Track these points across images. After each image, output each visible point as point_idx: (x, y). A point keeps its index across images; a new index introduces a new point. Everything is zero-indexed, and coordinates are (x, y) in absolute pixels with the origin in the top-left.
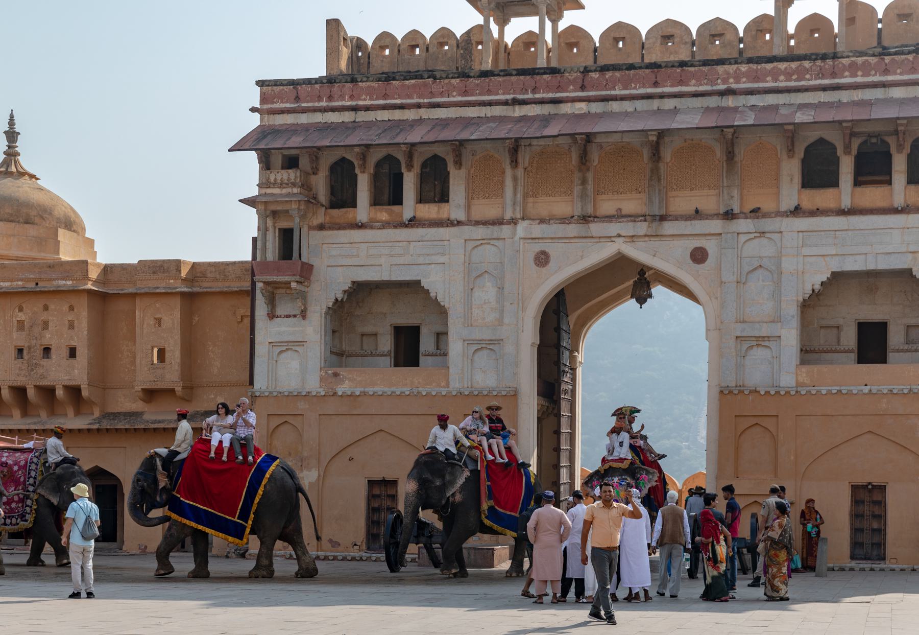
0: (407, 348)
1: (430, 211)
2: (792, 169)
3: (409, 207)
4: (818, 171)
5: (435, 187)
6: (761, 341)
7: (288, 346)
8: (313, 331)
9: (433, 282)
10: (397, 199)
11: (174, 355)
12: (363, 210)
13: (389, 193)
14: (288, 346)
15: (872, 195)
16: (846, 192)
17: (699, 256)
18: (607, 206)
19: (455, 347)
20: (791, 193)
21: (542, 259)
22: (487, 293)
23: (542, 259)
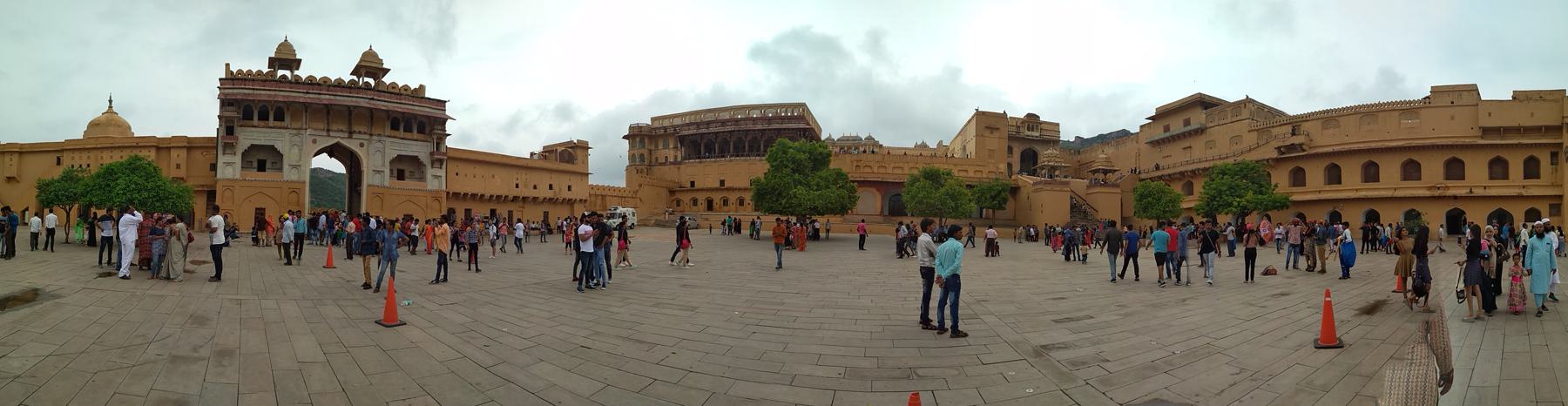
0: (262, 167)
1: (278, 124)
2: (388, 125)
3: (271, 122)
4: (395, 127)
5: (279, 117)
6: (378, 172)
7: (229, 164)
8: (238, 159)
9: (278, 146)
10: (267, 119)
11: (183, 166)
12: (256, 121)
13: (264, 117)
14: (229, 164)
15: (408, 135)
16: (401, 133)
17: (362, 145)
18: (334, 127)
19: (286, 167)
20: (388, 131)
21: (314, 142)
22: (296, 150)
23: (314, 142)
